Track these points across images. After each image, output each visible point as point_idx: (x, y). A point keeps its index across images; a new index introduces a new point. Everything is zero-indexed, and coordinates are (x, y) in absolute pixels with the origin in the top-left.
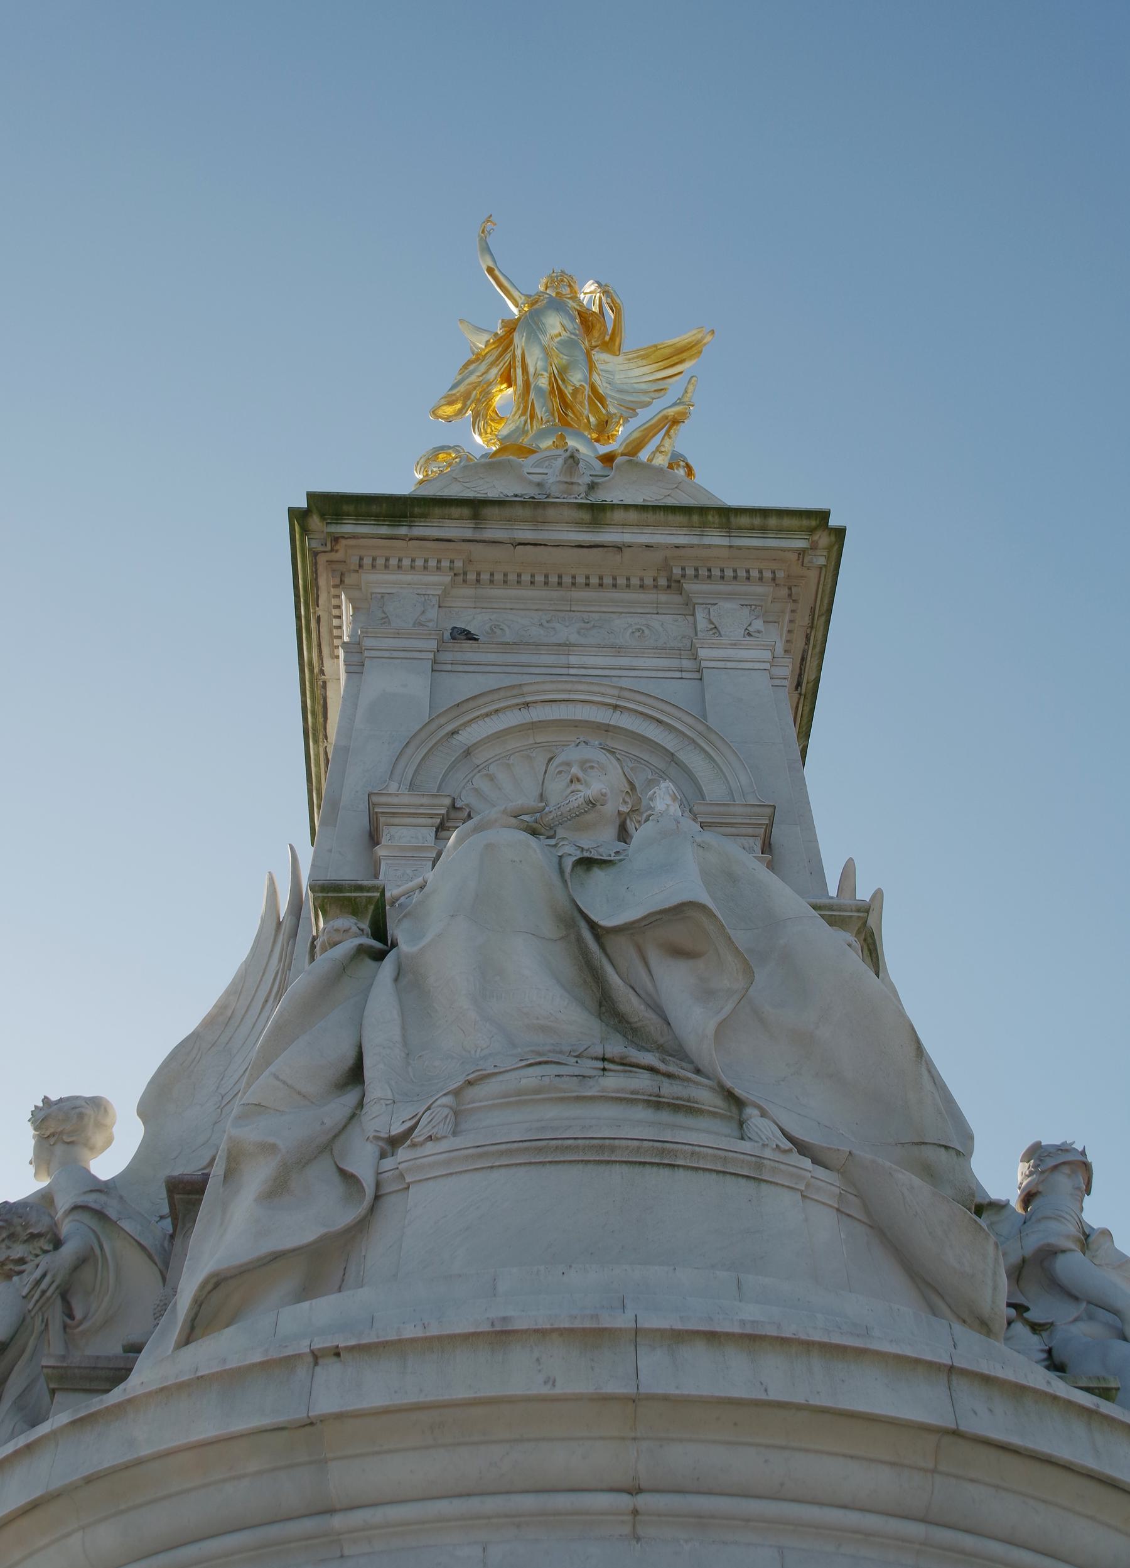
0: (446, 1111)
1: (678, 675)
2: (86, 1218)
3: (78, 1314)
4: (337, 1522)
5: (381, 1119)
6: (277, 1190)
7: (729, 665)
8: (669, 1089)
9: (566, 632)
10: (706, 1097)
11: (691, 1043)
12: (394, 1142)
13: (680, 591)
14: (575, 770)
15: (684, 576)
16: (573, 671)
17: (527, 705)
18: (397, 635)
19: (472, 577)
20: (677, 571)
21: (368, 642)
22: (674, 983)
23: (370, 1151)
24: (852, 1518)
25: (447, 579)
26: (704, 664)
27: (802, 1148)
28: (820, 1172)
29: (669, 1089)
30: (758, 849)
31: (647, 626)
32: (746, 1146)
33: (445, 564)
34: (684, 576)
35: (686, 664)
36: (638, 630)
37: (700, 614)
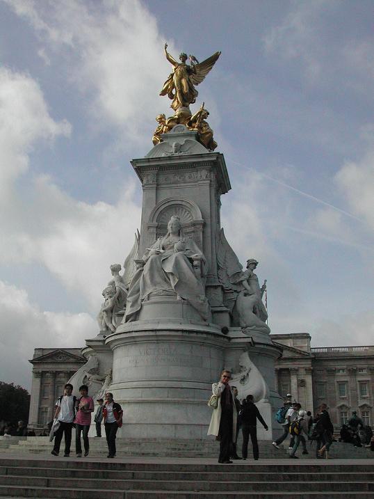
6: (132, 306)
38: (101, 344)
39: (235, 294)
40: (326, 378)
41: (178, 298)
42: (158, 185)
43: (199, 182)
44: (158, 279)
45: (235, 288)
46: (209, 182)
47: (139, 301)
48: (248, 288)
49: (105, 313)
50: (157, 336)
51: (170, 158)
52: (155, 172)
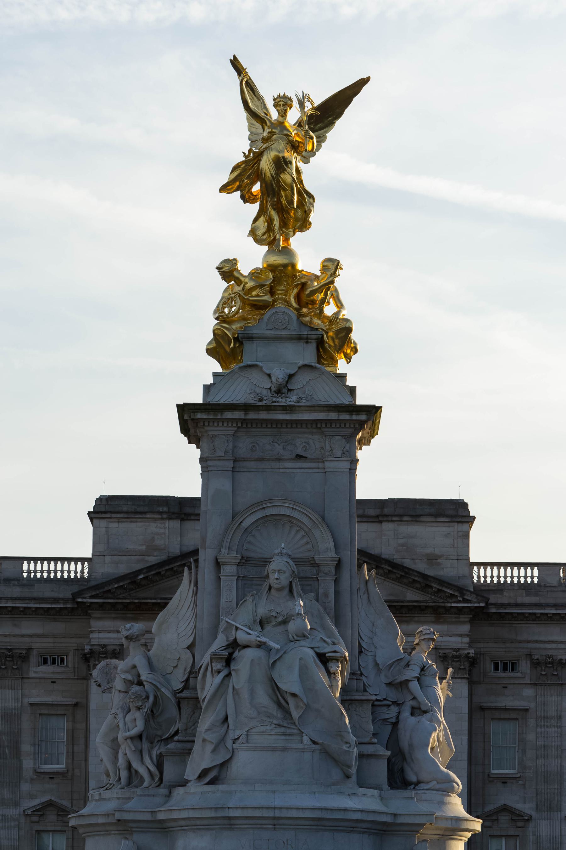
0: (245, 736)
1: (317, 471)
2: (152, 686)
3: (155, 712)
4: (233, 827)
5: (232, 735)
6: (214, 751)
7: (336, 470)
8: (288, 731)
9: (279, 449)
10: (295, 731)
11: (294, 718)
12: (235, 739)
13: (320, 428)
14: (276, 576)
15: (321, 425)
16: (281, 470)
17: (264, 508)
18: (220, 458)
19: (244, 426)
20: (319, 426)
21: (210, 463)
22: (291, 701)
23: (231, 742)
24: (306, 827)
25: (236, 429)
26: (327, 470)
27: (314, 742)
28: (317, 746)
29: (288, 731)
30: (334, 571)
31: (308, 443)
32: (301, 745)
33: (235, 425)
34: (321, 425)
35: (321, 465)
36: (305, 446)
37: (327, 443)
38: (148, 817)
39: (394, 710)
40: (529, 692)
41: (306, 739)
42: (235, 460)
43: (327, 464)
44: (263, 698)
45: (392, 695)
46: (348, 465)
47: (229, 744)
48: (421, 697)
49: (129, 741)
50: (274, 818)
51: (268, 408)
52: (231, 430)
